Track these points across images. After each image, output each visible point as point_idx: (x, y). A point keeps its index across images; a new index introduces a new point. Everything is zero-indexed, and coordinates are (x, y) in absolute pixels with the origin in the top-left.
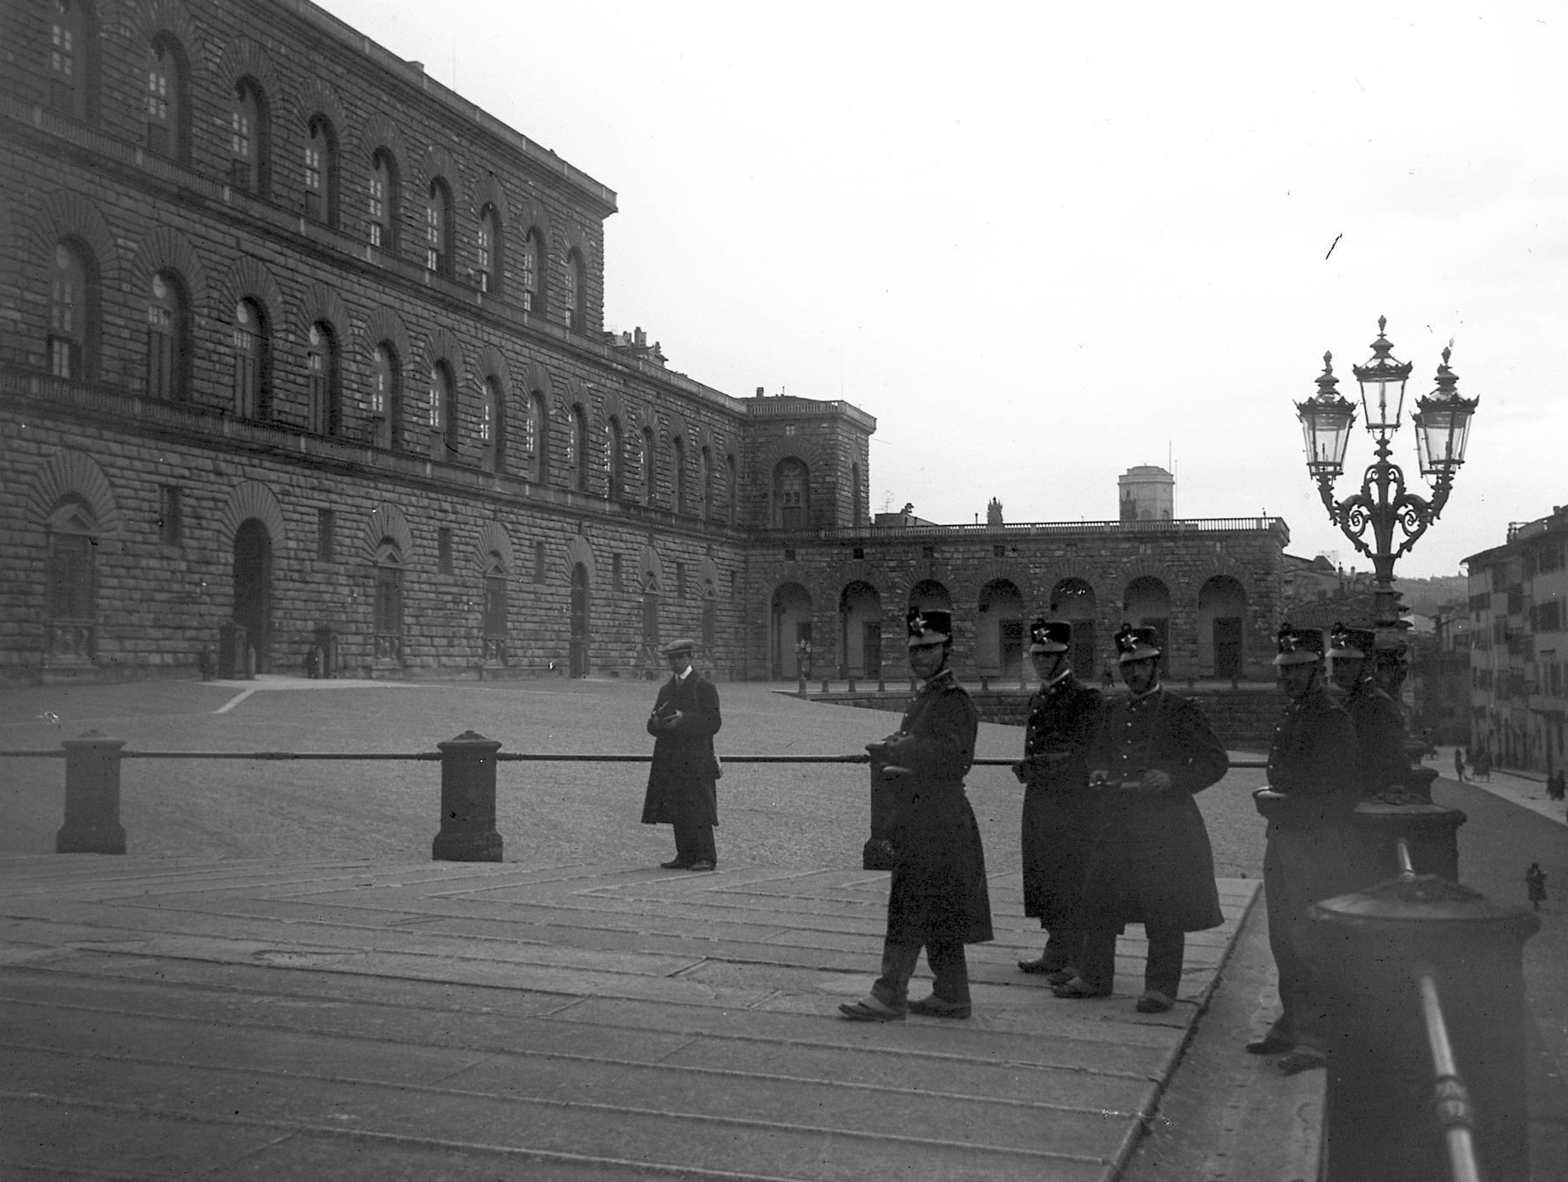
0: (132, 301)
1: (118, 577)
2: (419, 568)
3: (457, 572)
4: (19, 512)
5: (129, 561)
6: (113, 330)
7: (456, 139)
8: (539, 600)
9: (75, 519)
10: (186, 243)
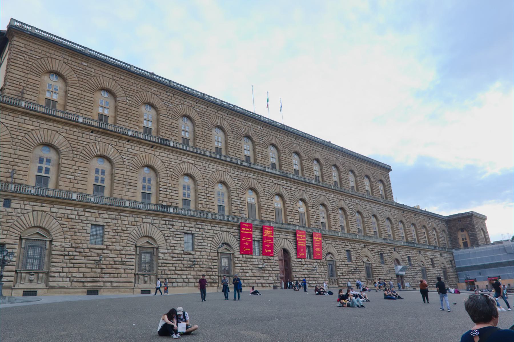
0: (240, 196)
1: (241, 264)
2: (341, 260)
4: (209, 248)
5: (244, 259)
6: (235, 203)
8: (383, 269)
9: (226, 249)
10: (256, 182)
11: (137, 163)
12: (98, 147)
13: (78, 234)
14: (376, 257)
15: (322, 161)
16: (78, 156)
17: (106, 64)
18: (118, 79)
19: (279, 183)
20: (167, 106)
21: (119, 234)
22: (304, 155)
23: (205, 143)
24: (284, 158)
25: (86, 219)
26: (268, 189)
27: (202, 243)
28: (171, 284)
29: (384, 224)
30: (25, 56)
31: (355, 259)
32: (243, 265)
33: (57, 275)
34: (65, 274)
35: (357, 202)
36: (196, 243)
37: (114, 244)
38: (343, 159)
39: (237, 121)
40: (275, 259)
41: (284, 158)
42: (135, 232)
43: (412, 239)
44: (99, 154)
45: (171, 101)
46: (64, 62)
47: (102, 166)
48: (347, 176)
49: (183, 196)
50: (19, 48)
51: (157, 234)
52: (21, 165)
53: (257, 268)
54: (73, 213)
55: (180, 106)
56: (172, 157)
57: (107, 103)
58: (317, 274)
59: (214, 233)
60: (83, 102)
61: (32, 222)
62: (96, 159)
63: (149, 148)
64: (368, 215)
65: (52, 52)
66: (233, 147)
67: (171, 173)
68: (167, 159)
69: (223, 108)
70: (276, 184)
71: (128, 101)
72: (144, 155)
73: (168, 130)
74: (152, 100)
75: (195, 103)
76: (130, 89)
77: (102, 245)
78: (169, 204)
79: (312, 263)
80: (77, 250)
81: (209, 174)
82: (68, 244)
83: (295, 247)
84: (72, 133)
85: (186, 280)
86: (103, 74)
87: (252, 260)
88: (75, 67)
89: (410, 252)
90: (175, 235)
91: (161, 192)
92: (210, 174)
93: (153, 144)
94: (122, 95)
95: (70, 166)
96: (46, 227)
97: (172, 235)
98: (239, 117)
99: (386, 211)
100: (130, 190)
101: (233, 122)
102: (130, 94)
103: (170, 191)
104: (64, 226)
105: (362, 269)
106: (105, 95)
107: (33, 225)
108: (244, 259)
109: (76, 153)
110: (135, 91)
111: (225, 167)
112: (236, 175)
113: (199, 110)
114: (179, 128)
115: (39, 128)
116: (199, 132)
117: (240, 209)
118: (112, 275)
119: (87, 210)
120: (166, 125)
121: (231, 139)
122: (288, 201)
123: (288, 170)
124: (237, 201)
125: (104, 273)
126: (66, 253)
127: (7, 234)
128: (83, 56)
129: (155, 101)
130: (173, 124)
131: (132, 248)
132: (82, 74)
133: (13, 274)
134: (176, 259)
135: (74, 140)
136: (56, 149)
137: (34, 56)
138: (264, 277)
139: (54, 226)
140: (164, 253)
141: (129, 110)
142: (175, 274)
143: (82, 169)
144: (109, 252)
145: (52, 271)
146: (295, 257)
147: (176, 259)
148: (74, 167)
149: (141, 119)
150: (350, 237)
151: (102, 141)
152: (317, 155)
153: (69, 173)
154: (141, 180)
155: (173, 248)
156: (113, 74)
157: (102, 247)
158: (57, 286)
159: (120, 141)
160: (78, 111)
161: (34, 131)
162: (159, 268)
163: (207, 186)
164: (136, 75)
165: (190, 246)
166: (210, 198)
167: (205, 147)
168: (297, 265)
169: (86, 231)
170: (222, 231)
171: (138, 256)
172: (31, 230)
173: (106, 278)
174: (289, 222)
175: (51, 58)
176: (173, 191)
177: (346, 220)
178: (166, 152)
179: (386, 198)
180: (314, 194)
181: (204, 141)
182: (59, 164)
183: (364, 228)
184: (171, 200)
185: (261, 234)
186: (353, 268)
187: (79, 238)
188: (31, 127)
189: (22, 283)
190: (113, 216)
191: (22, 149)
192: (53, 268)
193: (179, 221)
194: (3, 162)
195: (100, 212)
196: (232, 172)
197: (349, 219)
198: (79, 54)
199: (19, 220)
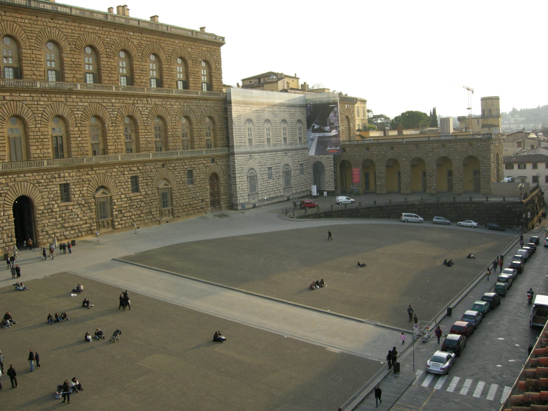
3: (141, 190)
19: (16, 99)
35: (157, 103)
58: (79, 219)
105: (154, 198)
122: (31, 125)
123: (34, 74)
177: (136, 133)
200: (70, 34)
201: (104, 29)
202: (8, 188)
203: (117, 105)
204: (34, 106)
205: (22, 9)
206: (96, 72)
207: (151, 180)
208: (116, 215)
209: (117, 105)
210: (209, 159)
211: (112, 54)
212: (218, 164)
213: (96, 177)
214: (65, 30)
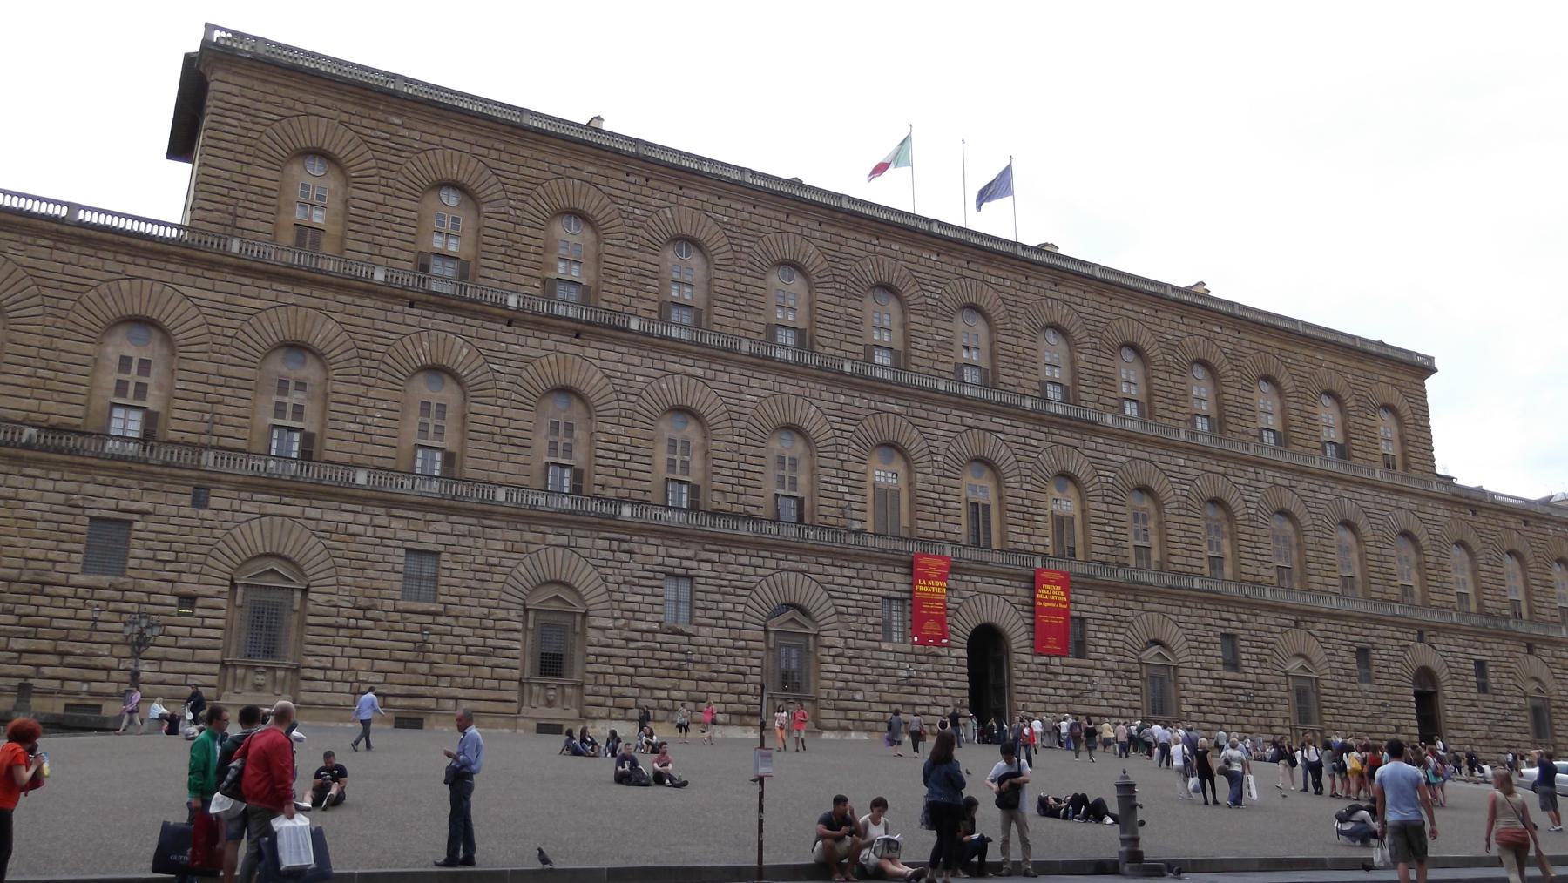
0: (848, 465)
1: (841, 665)
2: (1198, 665)
4: (740, 617)
7: (1219, 330)
9: (792, 620)
10: (905, 423)
11: (533, 383)
12: (426, 344)
13: (371, 574)
14: (1338, 659)
15: (1154, 351)
16: (373, 372)
17: (451, 114)
18: (485, 152)
20: (625, 215)
21: (479, 575)
22: (1085, 333)
23: (742, 315)
24: (1010, 347)
25: (392, 536)
26: (946, 445)
27: (717, 602)
28: (622, 711)
29: (1385, 552)
30: (242, 116)
31: (1254, 664)
32: (847, 668)
33: (319, 674)
34: (339, 673)
35: (1278, 481)
36: (699, 604)
37: (466, 601)
38: (1235, 341)
39: (851, 243)
40: (954, 653)
41: (1010, 347)
42: (522, 569)
43: (1500, 605)
44: (429, 362)
45: (639, 198)
46: (341, 122)
47: (438, 394)
48: (1247, 395)
49: (668, 471)
50: (226, 97)
51: (583, 576)
52: (232, 401)
53: (894, 680)
54: (361, 521)
55: (667, 210)
56: (637, 360)
57: (456, 220)
58: (1104, 703)
59: (756, 575)
60: (388, 225)
61: (259, 544)
62: (421, 377)
63: (567, 339)
64: (1319, 522)
65: (310, 98)
66: (832, 321)
67: (627, 405)
68: (621, 367)
69: (802, 206)
70: (973, 427)
71: (512, 212)
72: (552, 358)
73: (627, 283)
74: (582, 200)
75: (714, 199)
76: (518, 177)
77: (435, 602)
78: (624, 493)
79: (1089, 671)
80: (370, 614)
81: (750, 404)
82: (347, 598)
83: (1028, 621)
84: (357, 310)
85: (666, 704)
86: (446, 142)
87: (875, 654)
88: (369, 132)
89: (1488, 646)
90: (636, 580)
91: (601, 461)
92: (753, 405)
93: (579, 327)
94: (495, 197)
95: (353, 400)
96: (292, 555)
97: (627, 579)
98: (857, 228)
99: (1398, 508)
100: (513, 458)
101: (836, 247)
102: (520, 190)
103: (627, 457)
104: (338, 553)
105: (1279, 694)
106: (451, 198)
107: (261, 551)
108: (850, 653)
109: (367, 363)
110: (534, 180)
111: (804, 384)
112: (839, 406)
113: (726, 219)
114: (661, 275)
115: (275, 304)
116: (722, 283)
117: (845, 504)
118: (458, 680)
119: (395, 512)
120: (622, 268)
121: (826, 298)
122: (1013, 481)
124: (835, 481)
125: (438, 676)
126: (342, 621)
127: (200, 573)
128: (389, 99)
129: (590, 202)
130: (642, 265)
131: (513, 613)
132: (387, 150)
133: (216, 668)
134: (639, 644)
135: (365, 331)
136: (319, 356)
137: (264, 115)
138: (915, 704)
139: (313, 554)
140: (603, 629)
141: (516, 237)
142: (632, 686)
143: (385, 406)
144: (451, 621)
145: (307, 664)
146: (1027, 650)
147: (639, 644)
148: (363, 401)
149: (551, 258)
150: (1232, 590)
151: (437, 327)
152: (1130, 332)
153: (351, 418)
154: (545, 431)
155: (631, 614)
156: (472, 139)
157: (433, 607)
158: (320, 702)
159: (487, 325)
160: (377, 252)
161: (263, 313)
162: (590, 668)
163: (742, 440)
164: (536, 136)
165: (683, 610)
166: (749, 475)
167: (740, 328)
168: (1030, 675)
169: (393, 568)
170: (783, 570)
171: (530, 636)
172: (258, 563)
173: (444, 688)
174: (1011, 545)
175: (307, 114)
176: (635, 458)
178: (618, 349)
179: (1407, 465)
180: (1110, 456)
181: (737, 307)
182: (326, 395)
183: (1304, 563)
184: (629, 483)
185: (909, 579)
186: (1241, 691)
187: (376, 584)
188: (257, 303)
189: (237, 690)
190: (463, 529)
191: (236, 361)
192: (309, 658)
193: (651, 540)
194: (193, 396)
195: (430, 516)
196: (825, 395)
197: (1242, 536)
198: (380, 96)
199: (228, 538)
200: (1090, 317)
201: (1160, 314)
202: (961, 601)
203: (1188, 470)
204: (1018, 446)
205: (1000, 258)
206: (1143, 400)
207: (1269, 652)
208: (1188, 712)
209: (1188, 470)
210: (1412, 631)
211: (1176, 366)
212: (1433, 647)
213: (1144, 616)
214: (1078, 308)
